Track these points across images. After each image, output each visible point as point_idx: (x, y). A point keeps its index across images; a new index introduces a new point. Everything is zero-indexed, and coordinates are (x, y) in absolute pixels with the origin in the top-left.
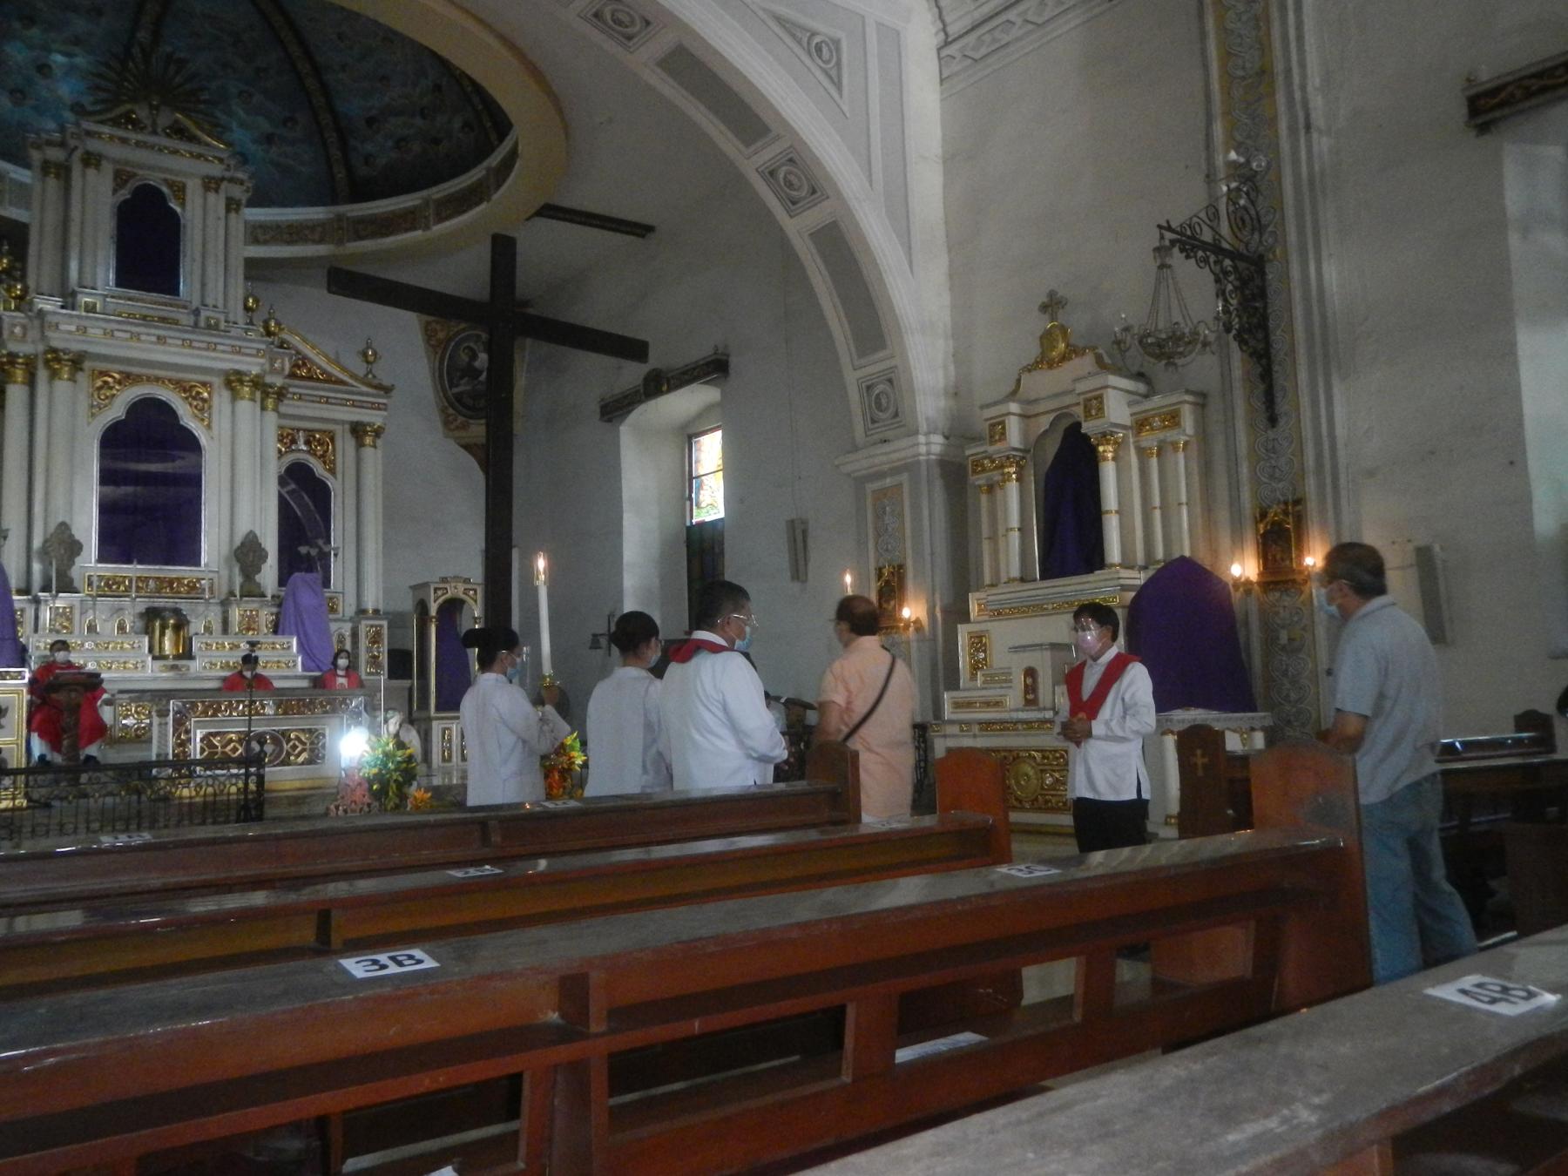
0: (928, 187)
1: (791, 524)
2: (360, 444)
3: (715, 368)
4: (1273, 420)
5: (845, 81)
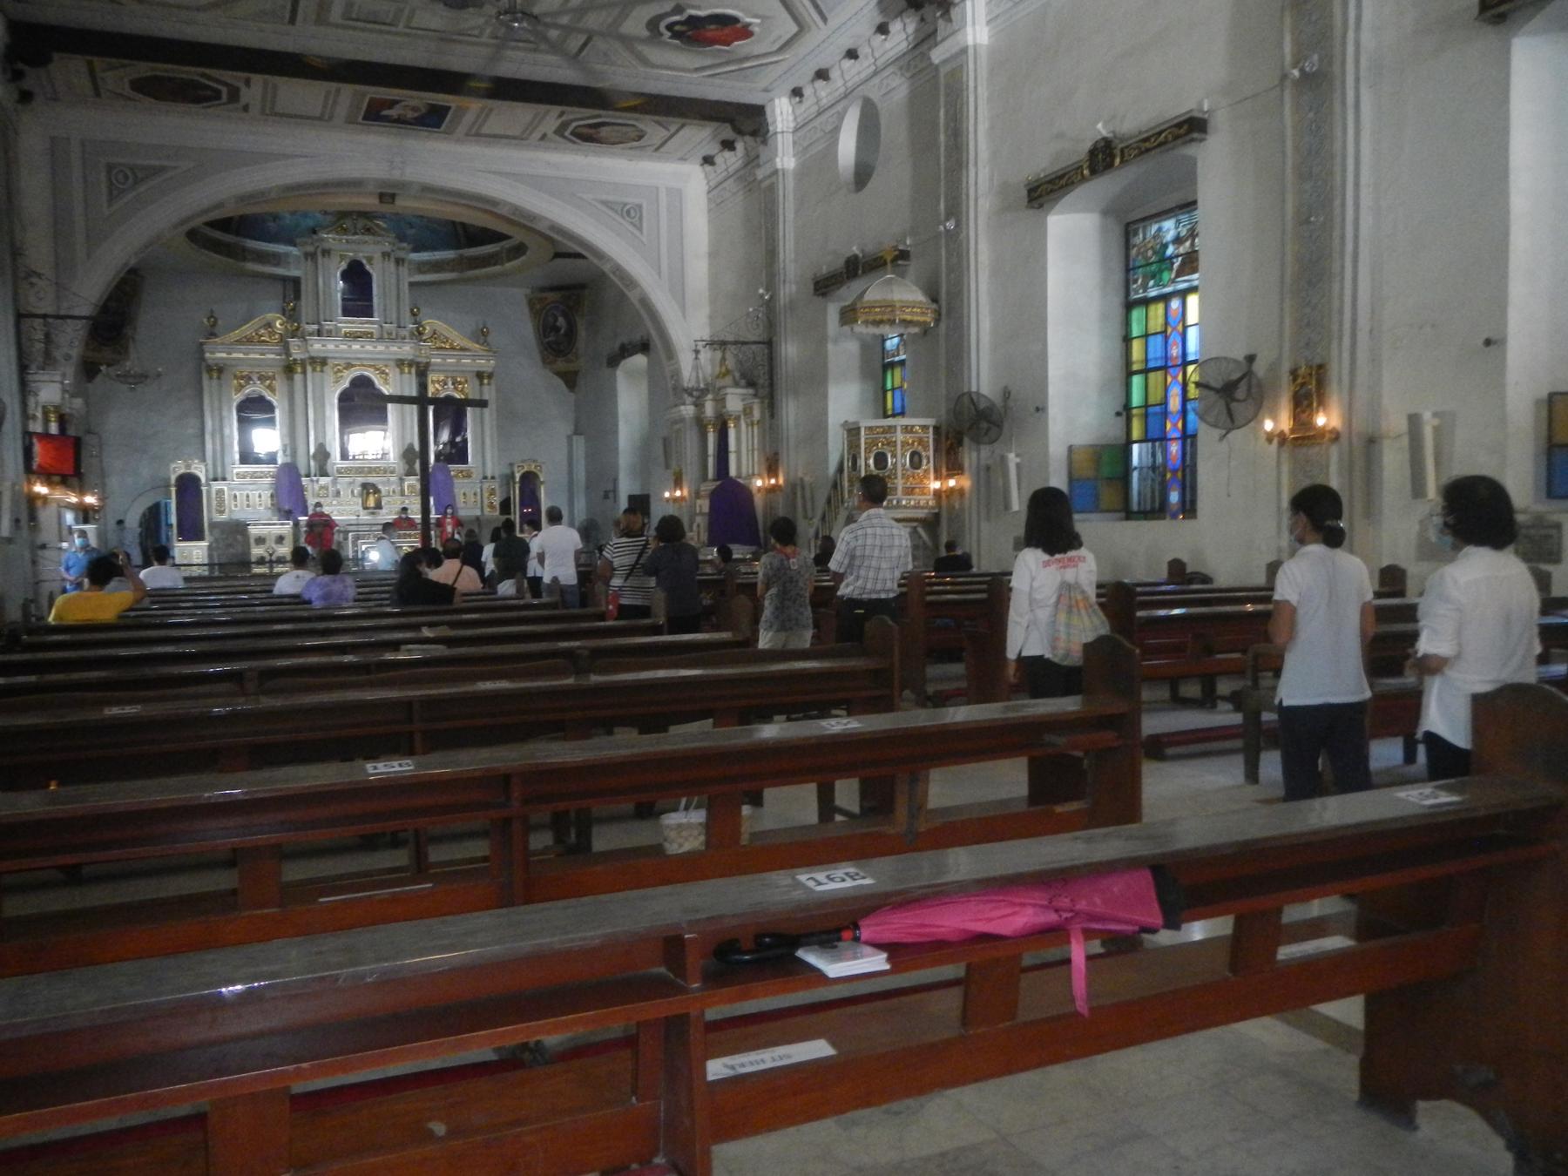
0: (698, 271)
1: (665, 440)
2: (482, 384)
3: (645, 347)
4: (772, 416)
5: (645, 225)
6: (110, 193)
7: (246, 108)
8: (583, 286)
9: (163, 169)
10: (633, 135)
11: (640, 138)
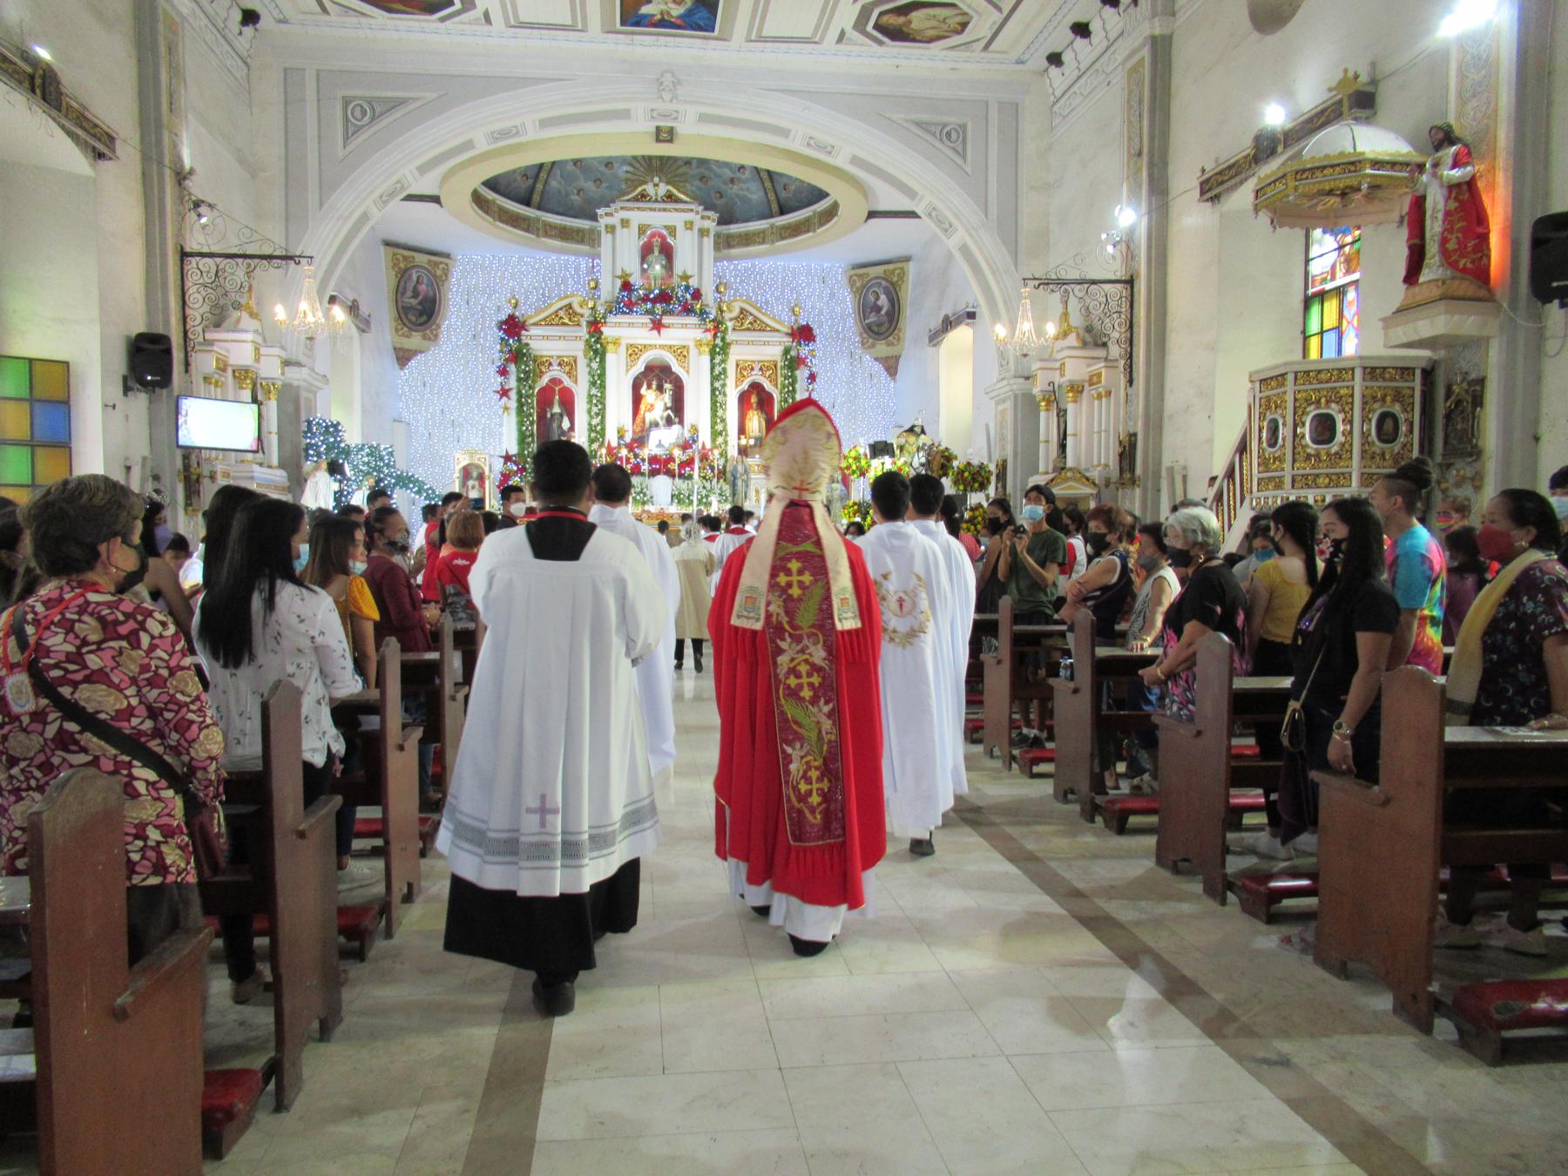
6: (346, 129)
7: (487, 16)
8: (907, 259)
9: (401, 102)
10: (954, 22)
11: (964, 25)
